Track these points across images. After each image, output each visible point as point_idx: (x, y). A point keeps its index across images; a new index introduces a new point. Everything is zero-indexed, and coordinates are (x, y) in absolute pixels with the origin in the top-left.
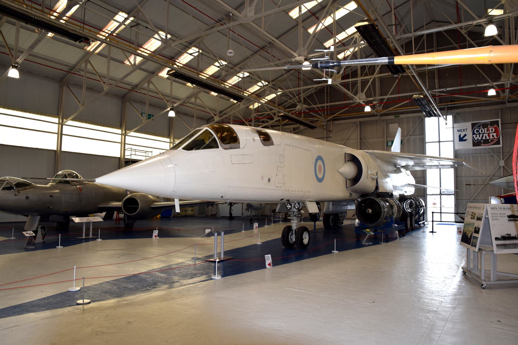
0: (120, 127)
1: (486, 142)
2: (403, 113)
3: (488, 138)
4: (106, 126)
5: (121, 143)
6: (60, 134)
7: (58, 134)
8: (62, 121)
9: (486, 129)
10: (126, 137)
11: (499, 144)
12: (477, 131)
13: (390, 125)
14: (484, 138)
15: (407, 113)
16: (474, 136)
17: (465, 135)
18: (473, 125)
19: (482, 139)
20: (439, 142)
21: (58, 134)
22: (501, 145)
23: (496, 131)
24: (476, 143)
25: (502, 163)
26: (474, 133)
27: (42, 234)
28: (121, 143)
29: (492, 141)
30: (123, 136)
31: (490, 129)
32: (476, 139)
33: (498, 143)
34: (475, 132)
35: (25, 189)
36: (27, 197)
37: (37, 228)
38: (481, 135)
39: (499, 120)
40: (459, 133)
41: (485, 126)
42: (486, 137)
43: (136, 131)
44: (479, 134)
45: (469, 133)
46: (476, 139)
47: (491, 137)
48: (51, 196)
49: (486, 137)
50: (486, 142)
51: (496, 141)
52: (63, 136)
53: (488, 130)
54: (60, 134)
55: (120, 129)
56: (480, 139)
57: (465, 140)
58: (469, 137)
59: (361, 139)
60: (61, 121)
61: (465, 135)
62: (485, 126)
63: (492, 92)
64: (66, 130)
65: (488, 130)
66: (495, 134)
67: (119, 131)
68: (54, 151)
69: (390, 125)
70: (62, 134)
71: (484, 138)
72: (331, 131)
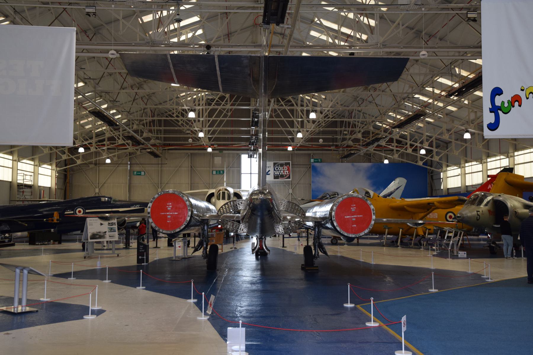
1: (282, 176)
2: (225, 150)
13: (215, 158)
15: (228, 150)
17: (269, 171)
18: (275, 164)
20: (251, 173)
22: (291, 179)
23: (288, 170)
24: (276, 177)
25: (291, 191)
26: (275, 170)
33: (289, 178)
41: (282, 165)
50: (282, 176)
51: (288, 176)
53: (283, 168)
59: (191, 167)
61: (269, 171)
62: (282, 165)
63: (290, 149)
65: (283, 168)
66: (287, 172)
69: (215, 158)
72: (167, 159)
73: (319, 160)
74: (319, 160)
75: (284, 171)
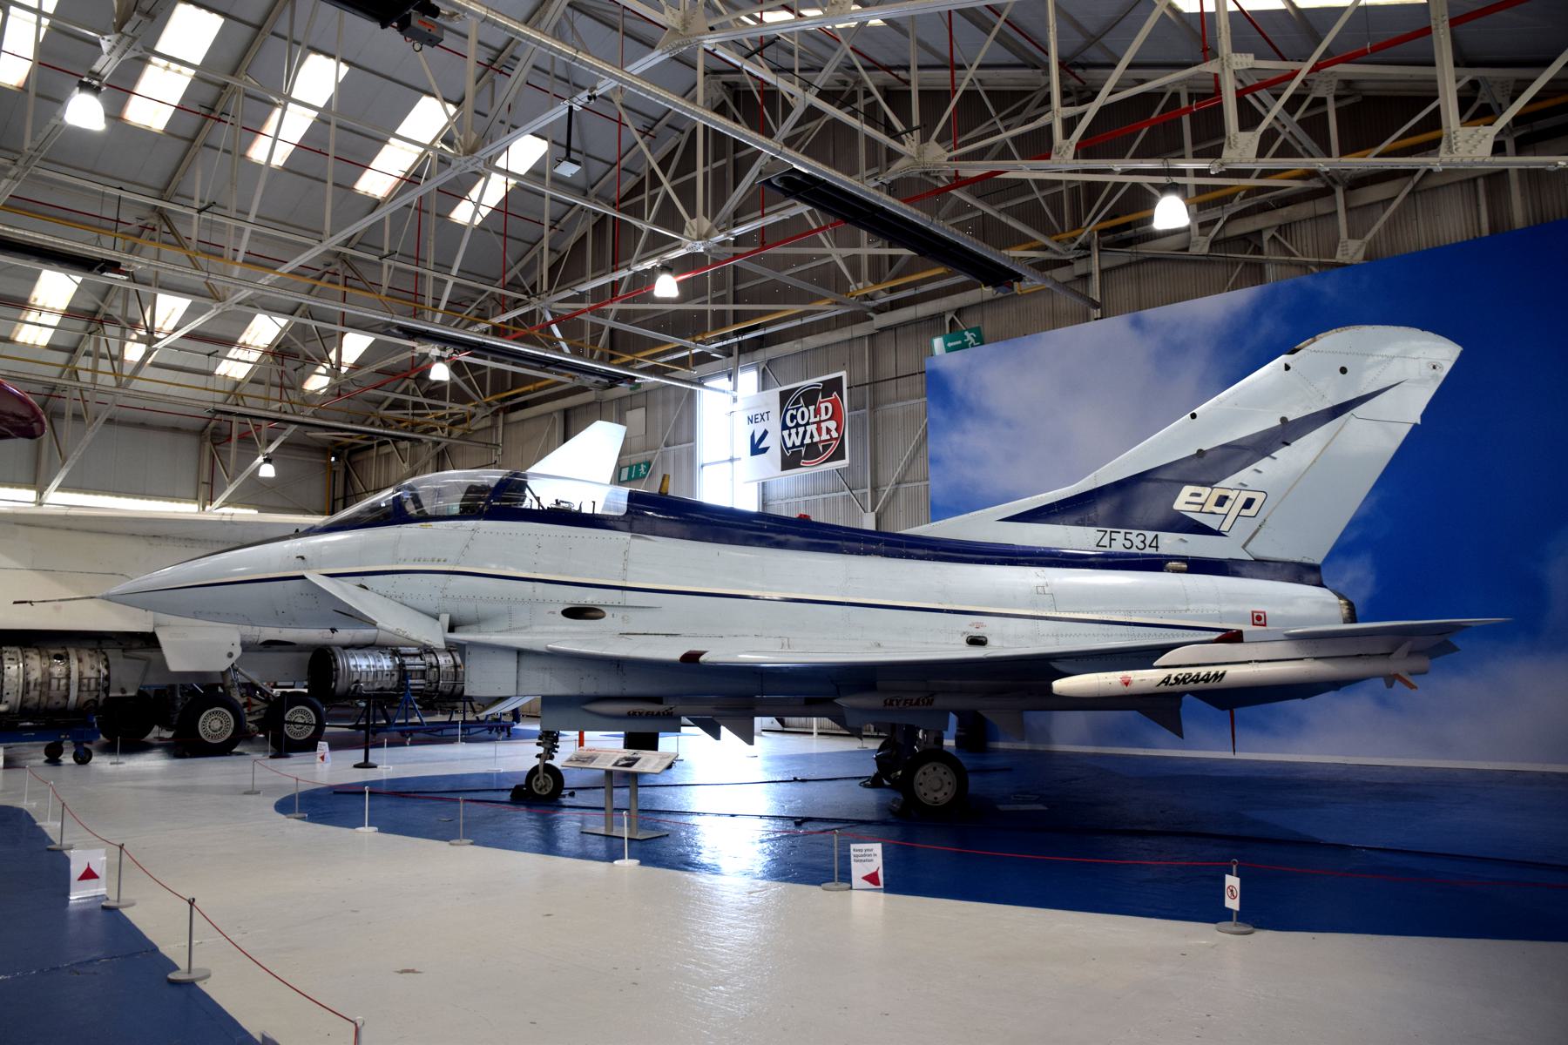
1: (812, 451)
3: (816, 439)
9: (812, 408)
11: (843, 457)
12: (793, 417)
14: (808, 441)
16: (786, 433)
17: (765, 433)
18: (784, 396)
19: (802, 444)
23: (836, 415)
24: (790, 460)
26: (784, 427)
29: (826, 448)
31: (823, 406)
32: (789, 444)
33: (839, 455)
34: (789, 424)
38: (801, 430)
39: (843, 374)
40: (753, 426)
41: (810, 397)
42: (812, 437)
44: (798, 425)
45: (774, 424)
46: (789, 444)
47: (825, 437)
49: (812, 437)
50: (812, 451)
53: (817, 412)
56: (798, 443)
57: (765, 450)
58: (773, 442)
61: (765, 433)
65: (817, 412)
66: (832, 425)
71: (808, 441)
73: (969, 336)
74: (969, 336)
75: (820, 425)
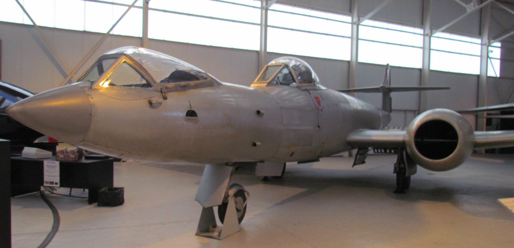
0: (349, 12)
4: (330, 11)
5: (352, 38)
6: (265, 26)
7: (261, 25)
8: (267, 4)
10: (360, 27)
21: (261, 25)
27: (238, 210)
28: (352, 38)
30: (355, 27)
35: (184, 88)
36: (191, 114)
37: (226, 197)
43: (372, 18)
48: (258, 112)
52: (268, 28)
54: (265, 26)
55: (349, 15)
60: (264, 4)
64: (273, 18)
67: (349, 19)
68: (257, 52)
70: (266, 26)
